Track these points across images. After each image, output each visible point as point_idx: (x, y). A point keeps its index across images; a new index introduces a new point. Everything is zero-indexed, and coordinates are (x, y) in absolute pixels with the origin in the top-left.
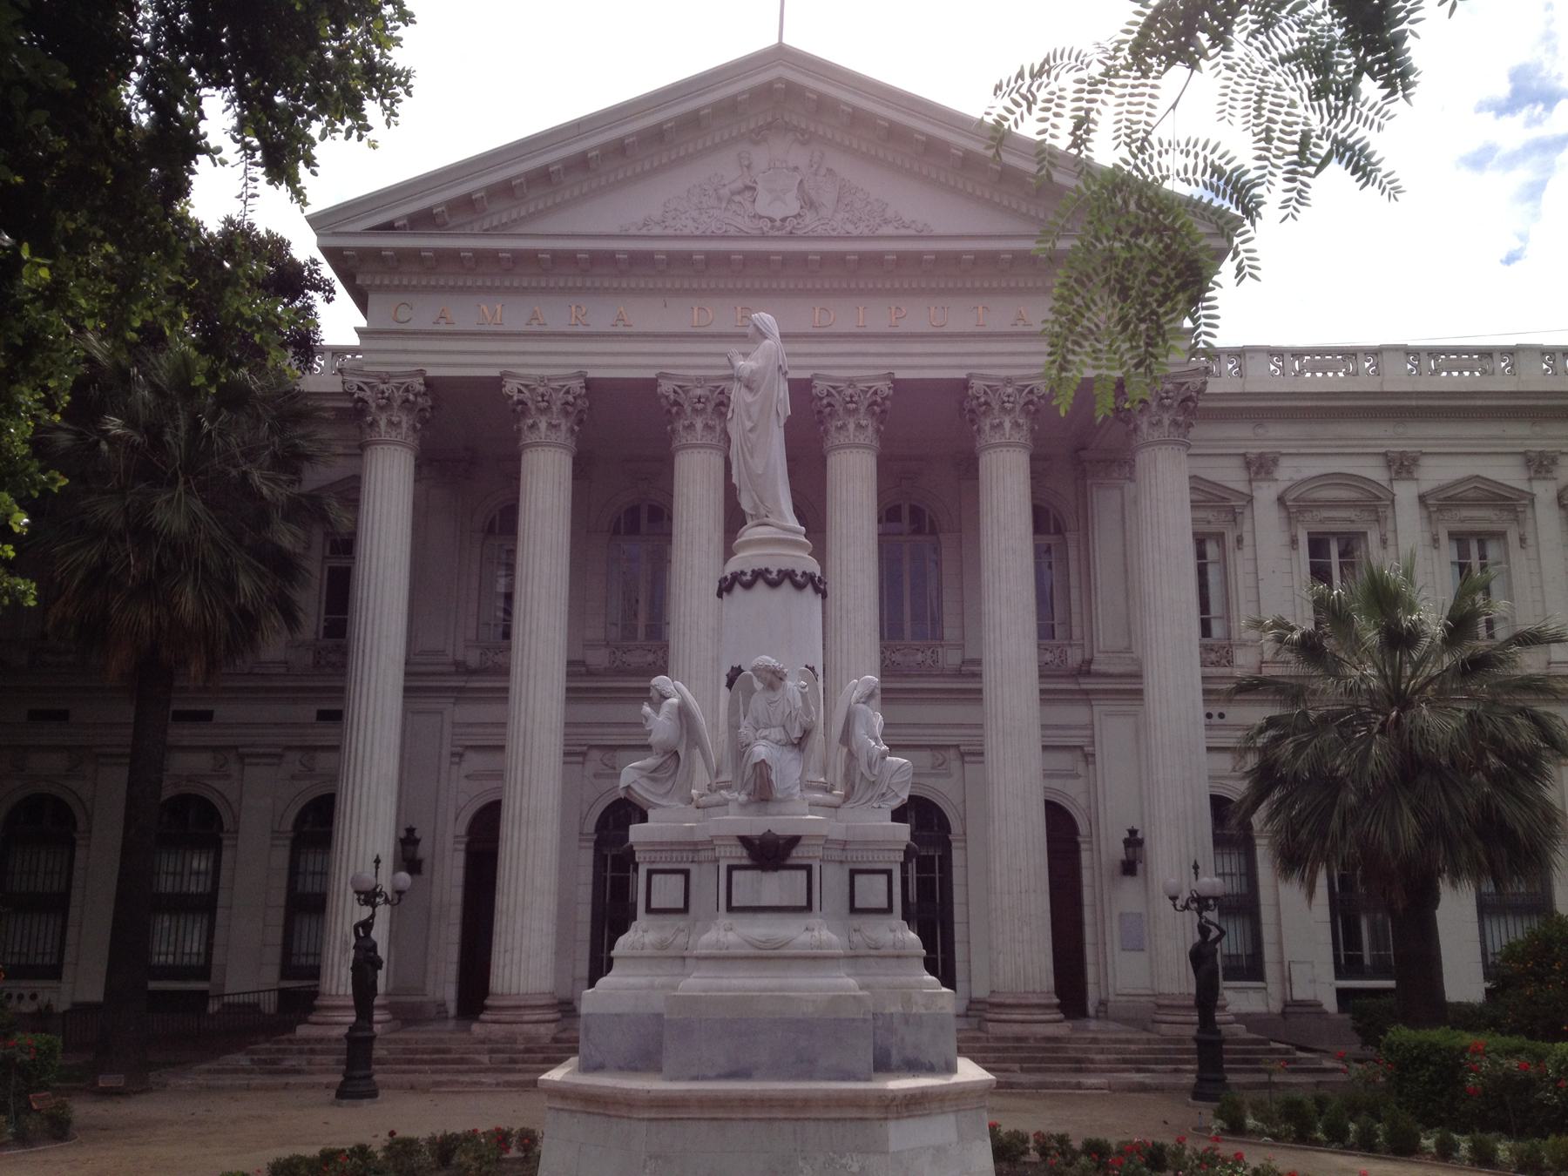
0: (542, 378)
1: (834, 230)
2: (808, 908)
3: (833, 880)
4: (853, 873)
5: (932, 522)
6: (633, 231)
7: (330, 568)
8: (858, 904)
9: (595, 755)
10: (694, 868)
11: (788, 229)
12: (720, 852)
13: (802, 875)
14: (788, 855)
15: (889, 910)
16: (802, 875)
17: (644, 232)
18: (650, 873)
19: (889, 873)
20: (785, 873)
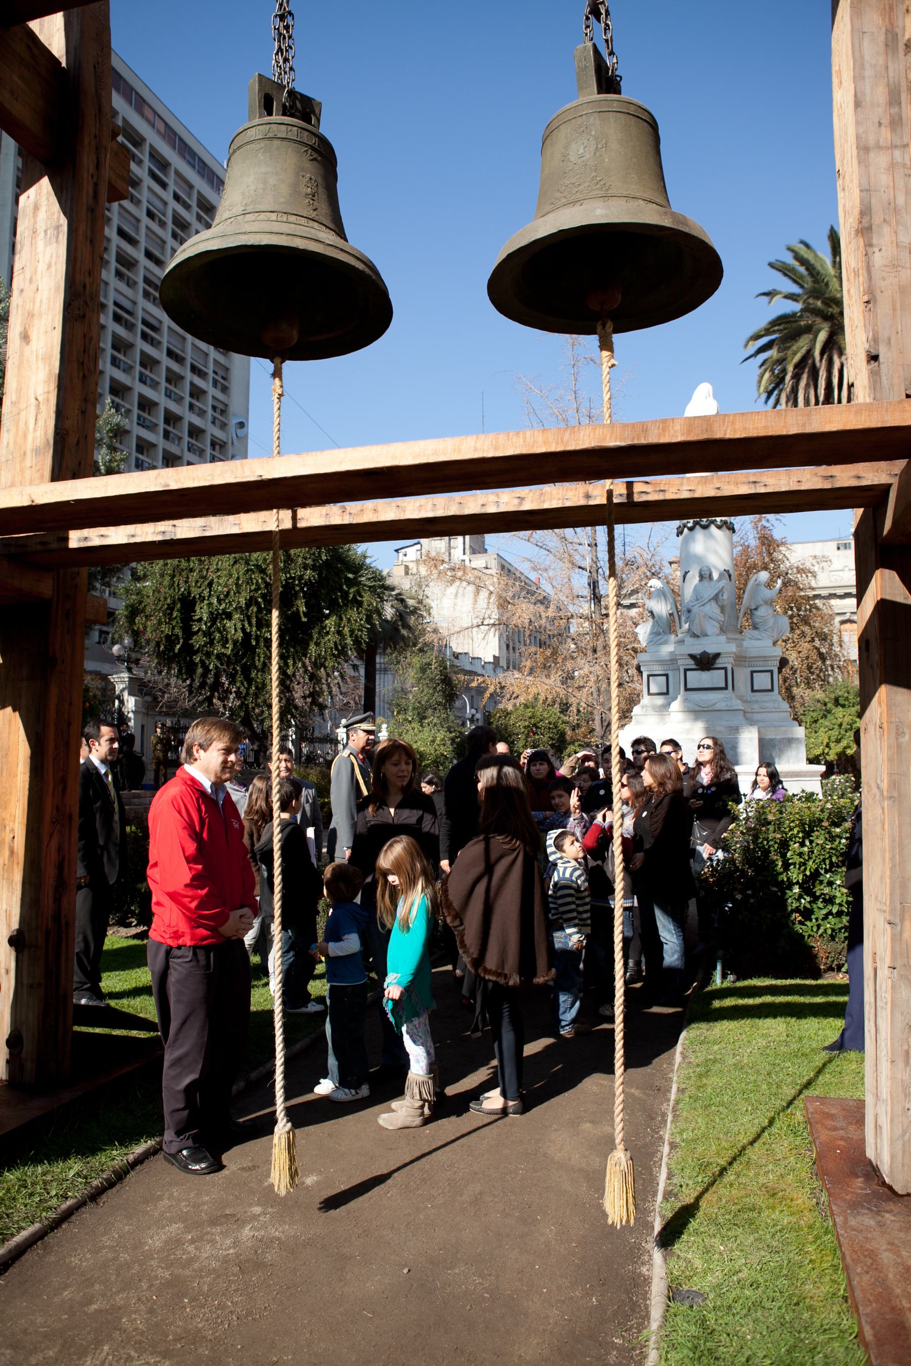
2: (726, 688)
3: (742, 676)
4: (752, 672)
8: (755, 688)
10: (670, 673)
12: (680, 662)
13: (723, 671)
14: (714, 663)
15: (772, 690)
16: (723, 671)
18: (649, 676)
19: (771, 672)
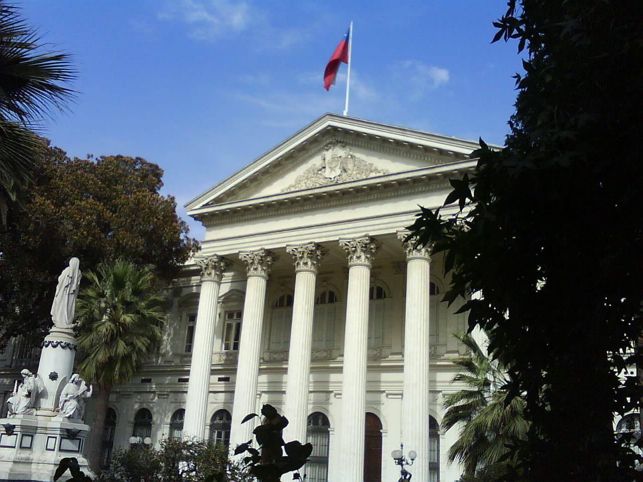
0: (251, 251)
1: (352, 178)
5: (437, 287)
6: (285, 192)
7: (228, 324)
9: (171, 395)
11: (335, 181)
17: (289, 191)
20: (12, 436)
